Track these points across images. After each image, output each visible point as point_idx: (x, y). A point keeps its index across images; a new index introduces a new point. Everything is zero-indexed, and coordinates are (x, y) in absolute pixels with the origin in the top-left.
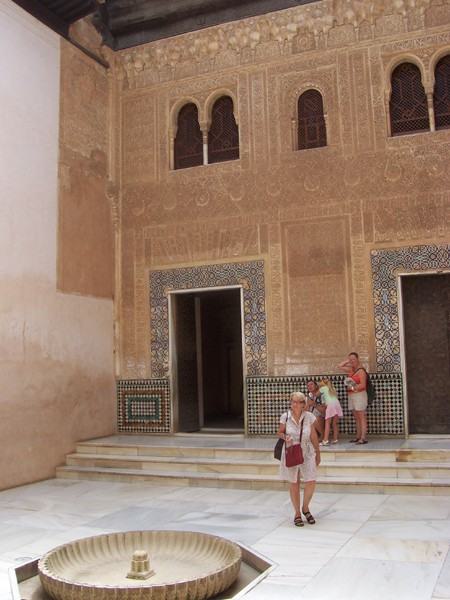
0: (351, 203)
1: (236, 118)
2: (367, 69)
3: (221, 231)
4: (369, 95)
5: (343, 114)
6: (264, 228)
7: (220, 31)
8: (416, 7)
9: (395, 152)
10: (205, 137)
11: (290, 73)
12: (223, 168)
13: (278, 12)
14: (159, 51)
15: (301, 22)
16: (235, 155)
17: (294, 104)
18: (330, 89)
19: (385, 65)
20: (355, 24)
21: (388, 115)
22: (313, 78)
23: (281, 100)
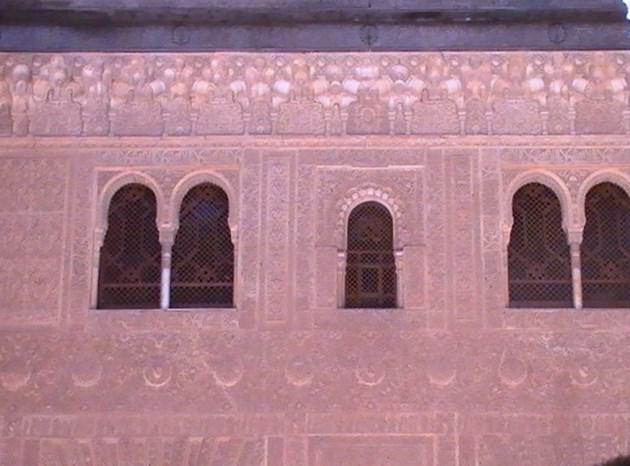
0: (439, 416)
1: (233, 229)
2: (476, 186)
3: (192, 440)
4: (478, 231)
5: (431, 256)
6: (276, 443)
7: (214, 63)
8: (562, 94)
9: (516, 336)
10: (167, 255)
11: (338, 167)
12: (200, 320)
13: (330, 54)
14: (88, 72)
15: (366, 79)
16: (223, 297)
17: (343, 222)
18: (408, 206)
19: (506, 184)
20: (460, 101)
21: (506, 269)
22: (380, 181)
23: (320, 211)
